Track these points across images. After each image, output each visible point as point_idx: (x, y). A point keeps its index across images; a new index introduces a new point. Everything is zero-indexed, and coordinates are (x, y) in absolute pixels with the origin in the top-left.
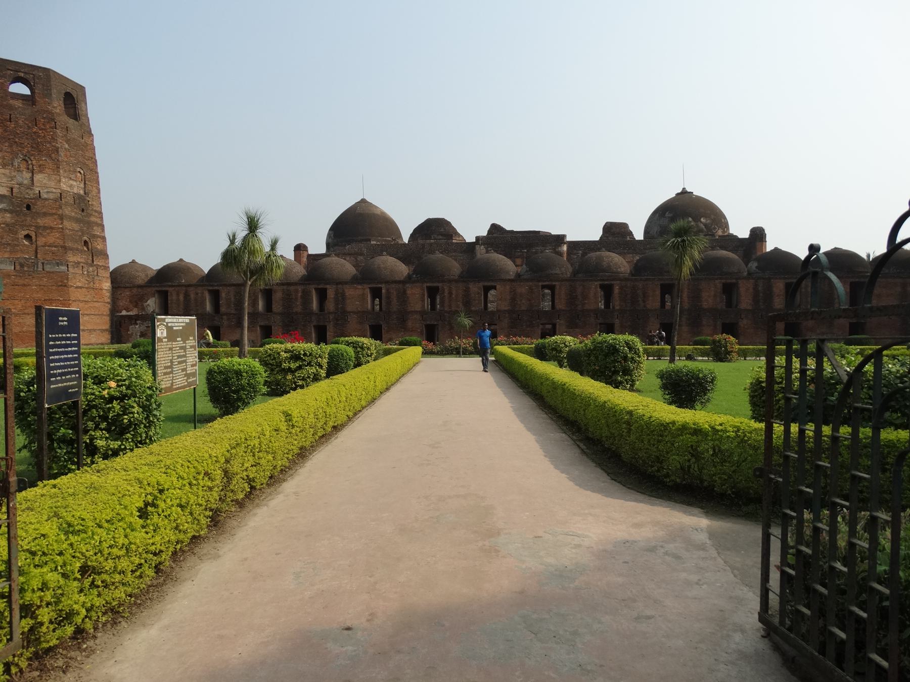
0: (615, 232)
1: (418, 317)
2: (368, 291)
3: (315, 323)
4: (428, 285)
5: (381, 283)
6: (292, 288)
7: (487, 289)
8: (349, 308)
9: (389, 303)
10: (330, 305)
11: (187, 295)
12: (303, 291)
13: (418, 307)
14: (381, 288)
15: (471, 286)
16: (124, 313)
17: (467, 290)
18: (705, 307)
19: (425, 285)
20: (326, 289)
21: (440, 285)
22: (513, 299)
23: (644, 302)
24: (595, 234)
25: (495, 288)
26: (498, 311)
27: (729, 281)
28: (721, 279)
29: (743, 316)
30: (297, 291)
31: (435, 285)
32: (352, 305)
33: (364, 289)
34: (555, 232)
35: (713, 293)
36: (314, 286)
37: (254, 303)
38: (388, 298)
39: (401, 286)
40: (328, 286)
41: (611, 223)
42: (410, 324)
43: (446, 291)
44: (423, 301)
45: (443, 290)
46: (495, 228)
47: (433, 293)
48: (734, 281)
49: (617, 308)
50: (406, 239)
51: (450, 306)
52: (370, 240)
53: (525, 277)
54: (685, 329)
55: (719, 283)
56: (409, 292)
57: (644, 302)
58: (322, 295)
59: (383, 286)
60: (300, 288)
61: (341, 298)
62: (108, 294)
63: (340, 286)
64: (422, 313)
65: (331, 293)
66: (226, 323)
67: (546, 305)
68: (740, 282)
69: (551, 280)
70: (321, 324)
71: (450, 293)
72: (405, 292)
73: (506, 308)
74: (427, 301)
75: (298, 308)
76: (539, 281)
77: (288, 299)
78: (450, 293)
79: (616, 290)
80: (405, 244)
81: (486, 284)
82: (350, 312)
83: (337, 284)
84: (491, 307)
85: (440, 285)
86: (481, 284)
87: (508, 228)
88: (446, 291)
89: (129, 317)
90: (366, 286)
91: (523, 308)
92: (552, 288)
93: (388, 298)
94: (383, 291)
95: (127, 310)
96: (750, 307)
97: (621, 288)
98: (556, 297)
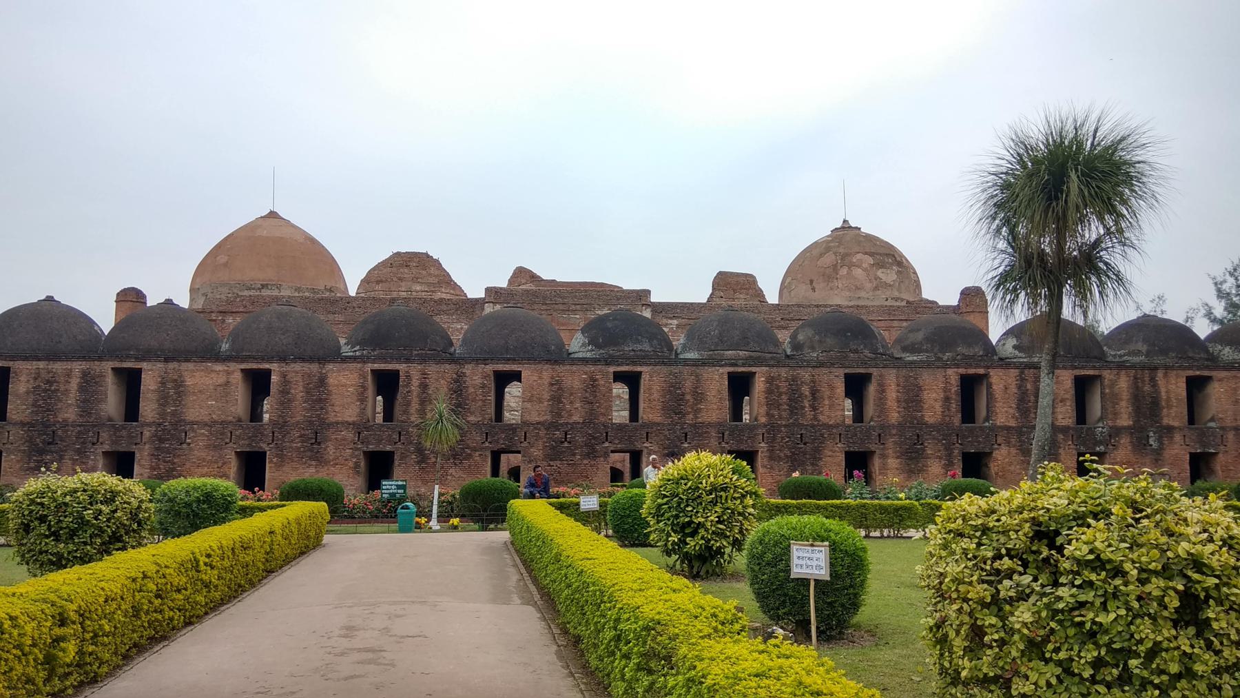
1: (349, 435)
2: (237, 377)
3: (107, 448)
4: (376, 366)
6: (58, 367)
7: (503, 380)
9: (286, 400)
10: (148, 408)
12: (85, 374)
13: (350, 413)
14: (268, 373)
15: (468, 369)
17: (459, 380)
19: (369, 367)
20: (139, 371)
21: (401, 367)
22: (557, 399)
25: (517, 376)
26: (525, 423)
27: (972, 371)
28: (958, 366)
29: (1000, 440)
30: (69, 374)
31: (390, 367)
32: (195, 411)
33: (228, 373)
34: (628, 285)
36: (108, 366)
38: (284, 392)
39: (314, 367)
40: (144, 365)
42: (331, 450)
43: (415, 382)
45: (408, 377)
47: (387, 384)
48: (981, 371)
49: (763, 420)
50: (352, 292)
51: (422, 412)
53: (580, 355)
54: (893, 462)
55: (953, 375)
56: (331, 381)
57: (814, 408)
58: (131, 382)
60: (78, 367)
61: (174, 391)
63: (171, 365)
64: (361, 428)
65: (149, 382)
68: (992, 372)
69: (634, 364)
70: (123, 448)
71: (424, 386)
72: (322, 381)
75: (69, 413)
76: (608, 364)
77: (47, 393)
78: (424, 386)
79: (759, 385)
80: (350, 300)
81: (501, 367)
82: (193, 423)
84: (511, 417)
85: (401, 367)
86: (490, 368)
87: (546, 276)
88: (415, 382)
90: (236, 369)
91: (576, 418)
92: (632, 381)
93: (284, 392)
94: (274, 378)
96: (1013, 423)
97: (770, 380)
98: (642, 396)
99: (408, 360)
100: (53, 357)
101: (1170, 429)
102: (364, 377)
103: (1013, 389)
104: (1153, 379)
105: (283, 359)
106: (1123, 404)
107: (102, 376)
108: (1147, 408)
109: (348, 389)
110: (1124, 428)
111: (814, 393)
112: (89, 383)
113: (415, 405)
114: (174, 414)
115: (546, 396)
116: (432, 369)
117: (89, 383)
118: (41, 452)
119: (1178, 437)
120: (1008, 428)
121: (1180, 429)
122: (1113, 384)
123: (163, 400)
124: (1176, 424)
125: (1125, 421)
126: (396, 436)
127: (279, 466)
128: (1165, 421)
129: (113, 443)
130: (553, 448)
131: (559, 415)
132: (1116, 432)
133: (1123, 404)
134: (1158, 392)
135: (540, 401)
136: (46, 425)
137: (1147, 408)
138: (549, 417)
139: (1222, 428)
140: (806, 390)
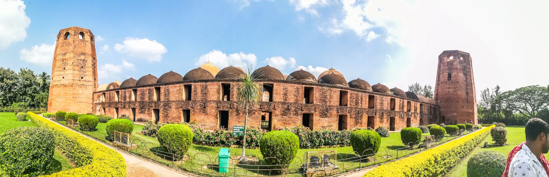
1: (214, 105)
5: (191, 82)
13: (215, 98)
19: (220, 83)
32: (172, 98)
38: (195, 91)
39: (204, 83)
42: (208, 110)
44: (219, 93)
56: (209, 87)
59: (192, 84)
65: (162, 91)
70: (157, 108)
73: (280, 101)
75: (147, 99)
83: (166, 84)
85: (231, 83)
99: (233, 81)
100: (144, 86)
102: (219, 86)
105: (195, 82)
107: (153, 89)
109: (214, 91)
112: (150, 92)
113: (235, 95)
114: (167, 99)
115: (282, 93)
116: (241, 83)
117: (150, 92)
118: (142, 109)
123: (165, 95)
126: (229, 106)
127: (193, 114)
129: (155, 106)
130: (284, 111)
131: (286, 100)
135: (280, 94)
136: (143, 102)
138: (282, 100)
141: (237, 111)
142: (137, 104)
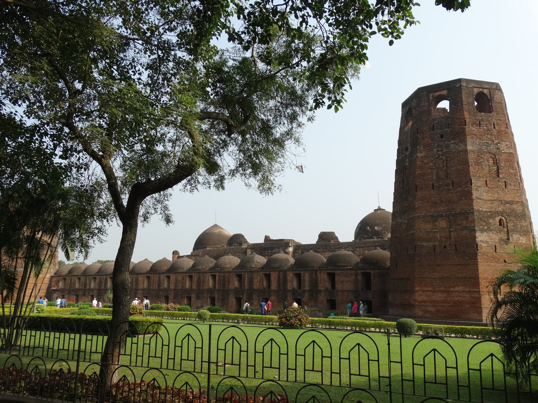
0: (327, 239)
6: (102, 277)
8: (139, 288)
11: (71, 280)
16: (53, 288)
18: (255, 288)
23: (228, 285)
24: (313, 240)
28: (262, 271)
35: (259, 280)
37: (90, 285)
39: (137, 276)
41: (323, 232)
46: (267, 238)
48: (268, 273)
52: (206, 248)
56: (139, 279)
62: (48, 280)
66: (80, 293)
67: (188, 285)
68: (271, 273)
74: (265, 283)
78: (154, 280)
89: (54, 290)
95: (54, 287)
96: (276, 289)
97: (219, 277)
101: (321, 291)
103: (277, 278)
104: (316, 274)
106: (307, 282)
108: (314, 284)
110: (306, 290)
111: (229, 280)
119: (322, 294)
120: (274, 290)
121: (323, 291)
122: (304, 275)
124: (323, 289)
125: (307, 288)
128: (319, 288)
132: (304, 291)
133: (307, 282)
134: (317, 278)
137: (314, 284)
139: (337, 291)
140: (226, 279)
141: (152, 296)
142: (95, 292)
